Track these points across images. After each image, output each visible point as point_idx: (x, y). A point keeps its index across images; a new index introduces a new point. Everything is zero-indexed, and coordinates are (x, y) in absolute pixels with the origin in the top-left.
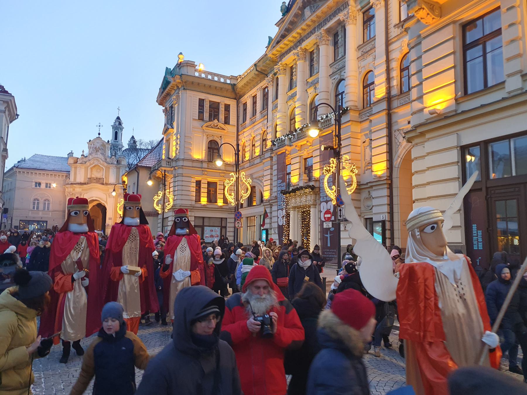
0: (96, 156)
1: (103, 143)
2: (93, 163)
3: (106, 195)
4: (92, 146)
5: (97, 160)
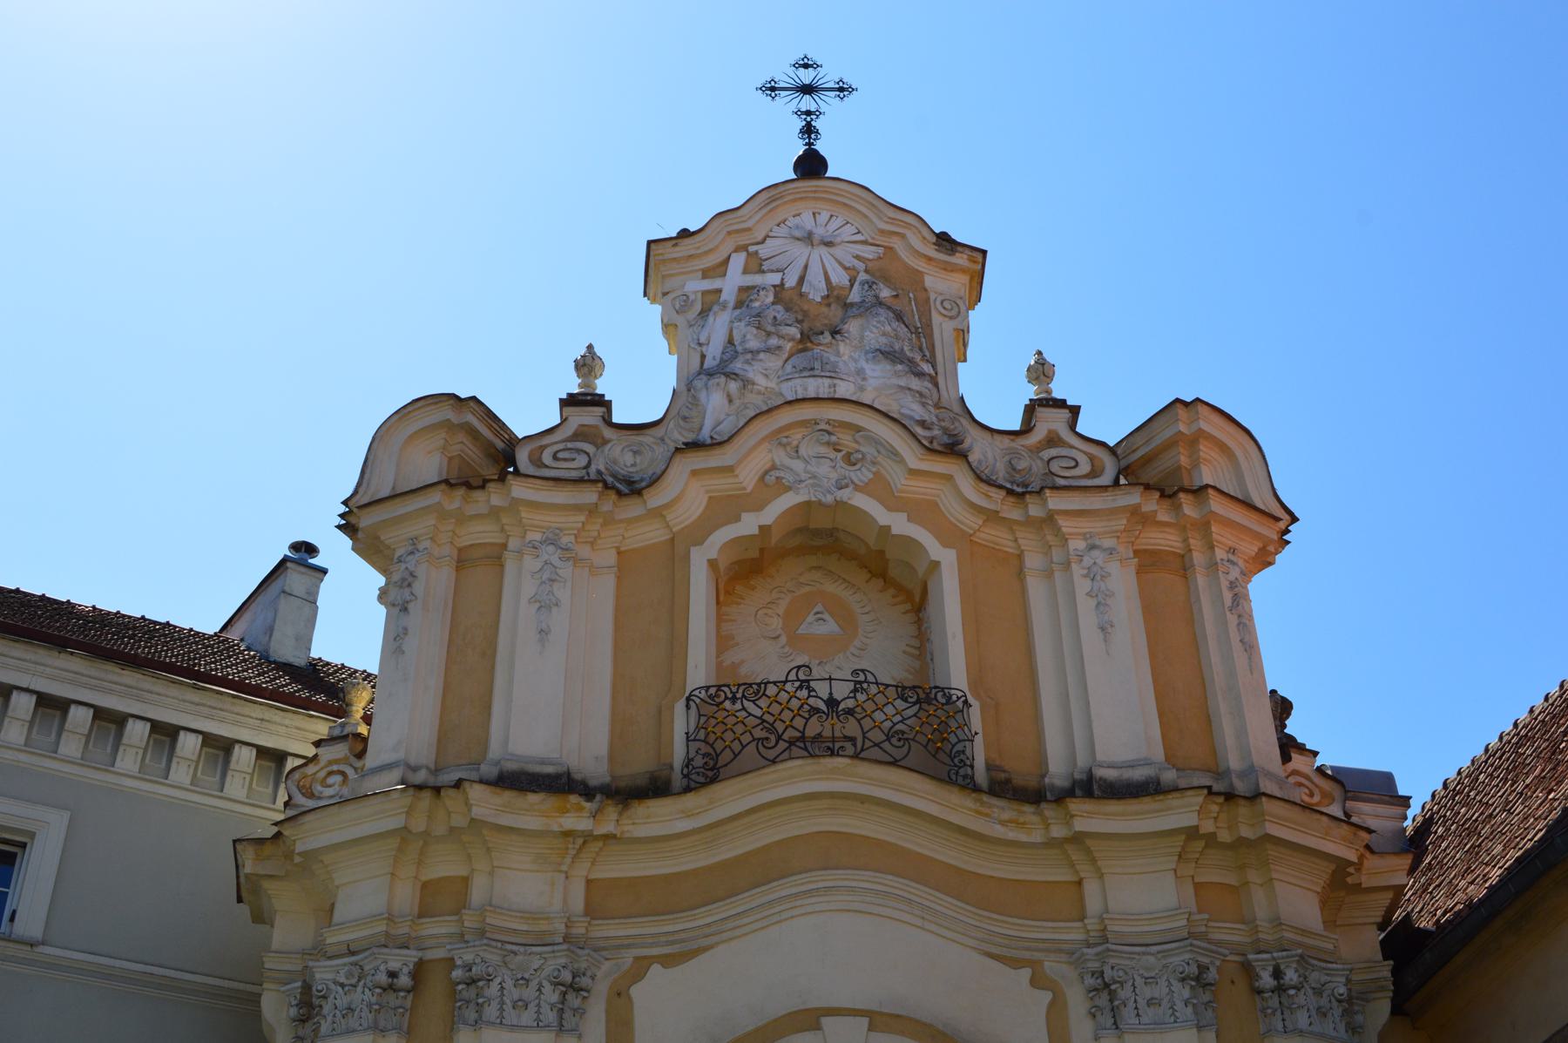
0: (815, 386)
1: (889, 249)
2: (772, 483)
4: (734, 279)
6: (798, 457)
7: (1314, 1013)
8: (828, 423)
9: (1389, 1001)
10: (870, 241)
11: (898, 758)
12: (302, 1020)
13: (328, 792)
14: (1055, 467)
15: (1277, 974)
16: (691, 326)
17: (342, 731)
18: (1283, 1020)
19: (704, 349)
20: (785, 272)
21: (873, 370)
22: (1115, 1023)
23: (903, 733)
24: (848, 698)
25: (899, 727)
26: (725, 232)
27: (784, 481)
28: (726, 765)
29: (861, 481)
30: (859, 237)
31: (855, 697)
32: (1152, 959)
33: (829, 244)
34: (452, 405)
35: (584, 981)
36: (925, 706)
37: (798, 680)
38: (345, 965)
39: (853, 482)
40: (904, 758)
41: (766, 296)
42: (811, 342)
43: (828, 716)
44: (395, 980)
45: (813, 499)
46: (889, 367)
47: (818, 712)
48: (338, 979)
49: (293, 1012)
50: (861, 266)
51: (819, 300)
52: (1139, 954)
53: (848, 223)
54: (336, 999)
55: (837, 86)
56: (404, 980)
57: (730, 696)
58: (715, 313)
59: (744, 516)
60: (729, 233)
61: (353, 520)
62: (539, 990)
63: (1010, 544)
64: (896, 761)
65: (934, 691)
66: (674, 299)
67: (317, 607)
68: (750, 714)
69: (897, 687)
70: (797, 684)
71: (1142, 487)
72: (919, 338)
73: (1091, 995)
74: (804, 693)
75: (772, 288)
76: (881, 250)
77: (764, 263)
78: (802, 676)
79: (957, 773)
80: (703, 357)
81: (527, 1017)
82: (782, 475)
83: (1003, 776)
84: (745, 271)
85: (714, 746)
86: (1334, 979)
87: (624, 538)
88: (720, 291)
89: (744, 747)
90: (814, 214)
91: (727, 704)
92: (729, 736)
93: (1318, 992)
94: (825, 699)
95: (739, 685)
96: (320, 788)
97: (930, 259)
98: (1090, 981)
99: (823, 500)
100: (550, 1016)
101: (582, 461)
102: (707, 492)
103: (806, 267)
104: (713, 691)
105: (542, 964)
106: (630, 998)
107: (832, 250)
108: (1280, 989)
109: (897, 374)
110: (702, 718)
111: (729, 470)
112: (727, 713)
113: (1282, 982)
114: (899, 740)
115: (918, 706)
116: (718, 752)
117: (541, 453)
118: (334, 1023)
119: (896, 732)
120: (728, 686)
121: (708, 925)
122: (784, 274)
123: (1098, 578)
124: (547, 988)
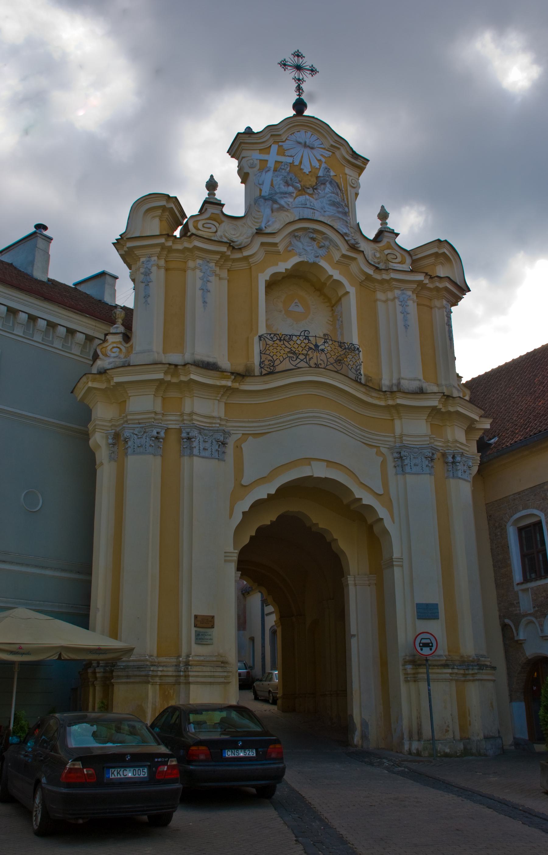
0: (307, 214)
3: (379, 453)
4: (272, 157)
5: (315, 231)
6: (300, 241)
7: (463, 471)
8: (313, 229)
9: (478, 467)
10: (327, 149)
11: (339, 369)
12: (114, 444)
13: (113, 355)
14: (389, 257)
15: (454, 457)
16: (255, 175)
17: (117, 331)
18: (453, 473)
19: (261, 186)
20: (294, 157)
21: (329, 208)
22: (402, 470)
23: (341, 360)
24: (322, 345)
25: (339, 358)
26: (269, 135)
27: (294, 251)
28: (277, 365)
29: (323, 255)
30: (322, 146)
31: (324, 345)
32: (416, 450)
33: (312, 148)
34: (166, 199)
35: (227, 441)
36: (347, 350)
37: (305, 336)
38: (138, 427)
39: (320, 255)
40: (341, 370)
41: (287, 168)
42: (305, 191)
43: (315, 351)
44: (159, 435)
45: (306, 260)
46: (335, 208)
47: (312, 349)
48: (135, 432)
49: (110, 441)
50: (323, 160)
51: (308, 173)
52: (413, 447)
53: (318, 139)
54: (134, 439)
55: (310, 68)
56: (162, 434)
57: (279, 338)
58: (266, 172)
59: (280, 263)
60: (272, 135)
61: (121, 242)
62: (212, 443)
63: (373, 287)
64: (338, 371)
65: (351, 345)
66: (248, 160)
67: (49, 255)
68: (286, 347)
69: (338, 342)
70: (304, 337)
71: (425, 274)
72: (343, 195)
73: (396, 460)
74: (306, 341)
75: (289, 164)
76: (331, 154)
77: (286, 152)
78: (306, 335)
79: (358, 377)
80: (261, 190)
81: (207, 454)
82: (294, 248)
83: (370, 378)
84: (278, 154)
85: (273, 357)
86: (469, 460)
87: (231, 266)
88: (267, 161)
89: (284, 359)
90: (305, 132)
91: (278, 342)
92: (278, 354)
93: (464, 465)
94: (314, 344)
95: (283, 335)
96: (109, 353)
97: (348, 161)
98: (396, 455)
99: (310, 261)
100: (216, 455)
101: (214, 229)
102: (265, 251)
103: (302, 157)
104: (272, 335)
105: (213, 434)
106: (241, 448)
107: (313, 151)
108: (454, 463)
109: (339, 212)
110: (267, 345)
111: (275, 245)
112: (277, 345)
113: (455, 460)
114: (339, 363)
115: (345, 350)
116: (275, 360)
117: (198, 223)
118: (134, 448)
119: (338, 360)
120: (278, 334)
121: (270, 425)
122: (294, 159)
123: (405, 306)
124: (215, 443)
